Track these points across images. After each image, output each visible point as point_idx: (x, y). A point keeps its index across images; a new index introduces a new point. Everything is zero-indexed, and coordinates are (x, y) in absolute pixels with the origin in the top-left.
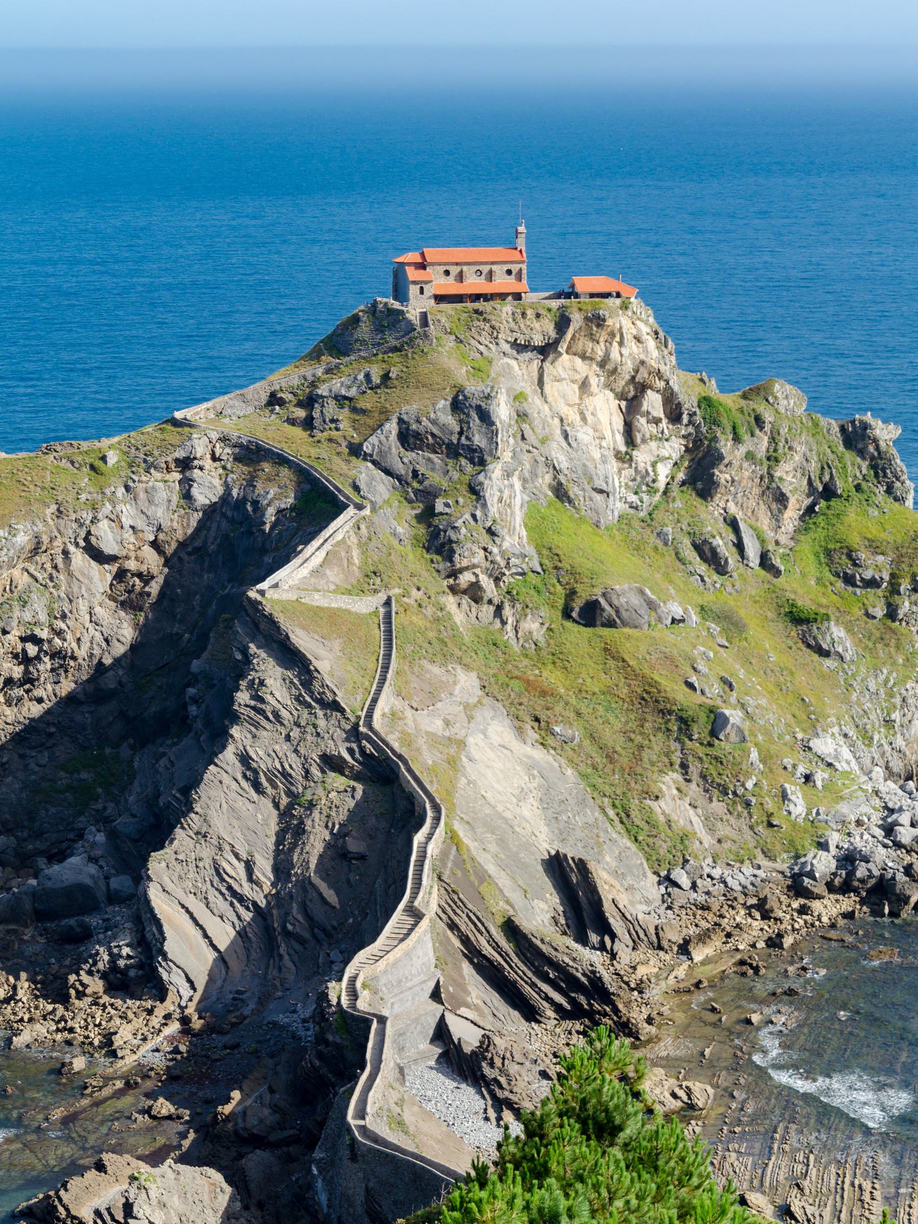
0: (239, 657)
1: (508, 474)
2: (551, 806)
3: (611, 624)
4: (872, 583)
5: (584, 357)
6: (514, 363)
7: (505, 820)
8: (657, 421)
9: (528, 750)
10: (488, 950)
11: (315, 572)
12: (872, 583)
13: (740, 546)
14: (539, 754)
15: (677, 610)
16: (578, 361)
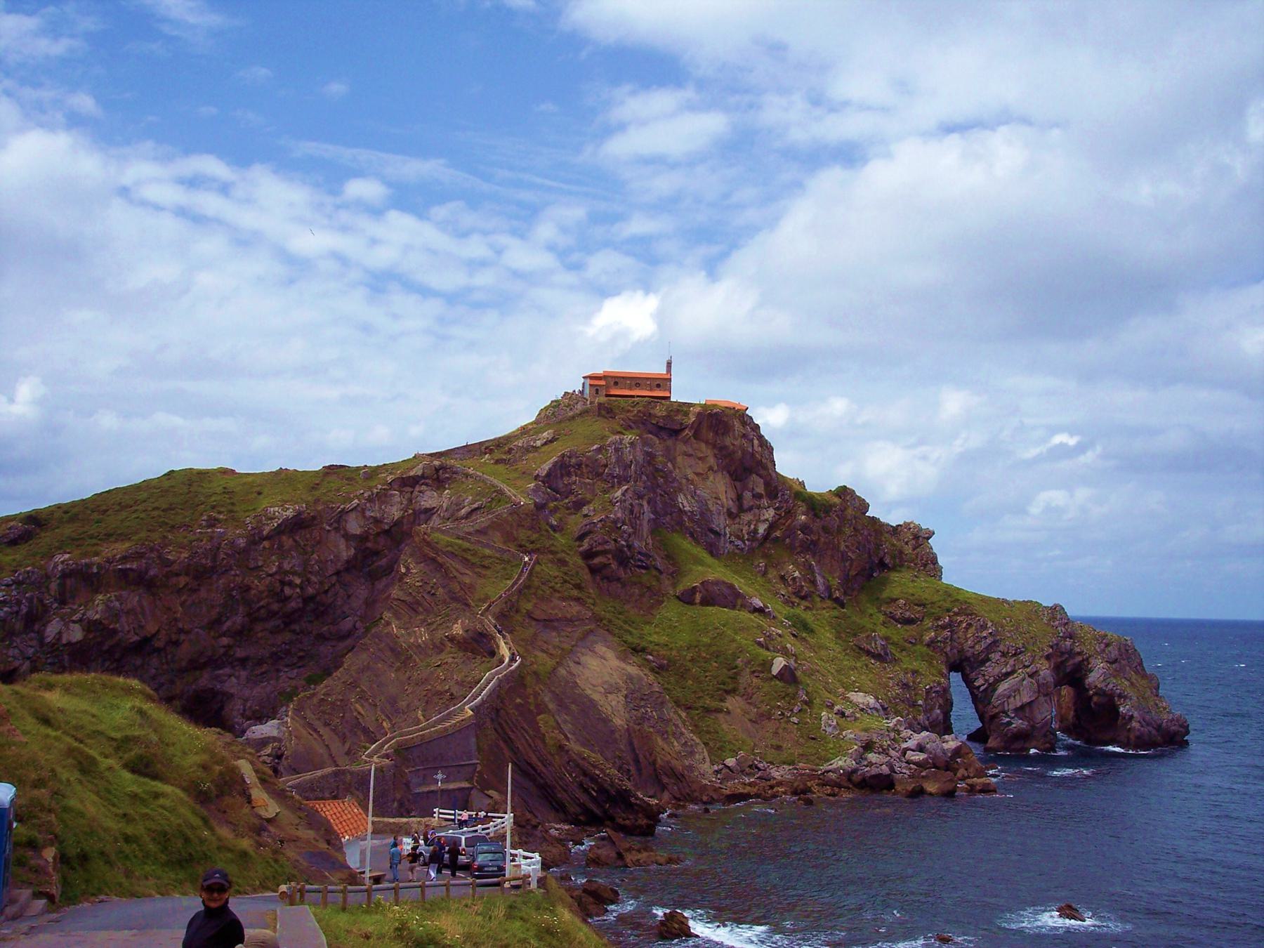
0: (403, 570)
1: (640, 497)
2: (635, 697)
3: (706, 602)
4: (909, 621)
5: (707, 443)
6: (655, 439)
7: (591, 701)
8: (759, 496)
9: (623, 665)
10: (534, 760)
12: (909, 621)
13: (813, 582)
14: (632, 670)
15: (758, 603)
16: (703, 446)
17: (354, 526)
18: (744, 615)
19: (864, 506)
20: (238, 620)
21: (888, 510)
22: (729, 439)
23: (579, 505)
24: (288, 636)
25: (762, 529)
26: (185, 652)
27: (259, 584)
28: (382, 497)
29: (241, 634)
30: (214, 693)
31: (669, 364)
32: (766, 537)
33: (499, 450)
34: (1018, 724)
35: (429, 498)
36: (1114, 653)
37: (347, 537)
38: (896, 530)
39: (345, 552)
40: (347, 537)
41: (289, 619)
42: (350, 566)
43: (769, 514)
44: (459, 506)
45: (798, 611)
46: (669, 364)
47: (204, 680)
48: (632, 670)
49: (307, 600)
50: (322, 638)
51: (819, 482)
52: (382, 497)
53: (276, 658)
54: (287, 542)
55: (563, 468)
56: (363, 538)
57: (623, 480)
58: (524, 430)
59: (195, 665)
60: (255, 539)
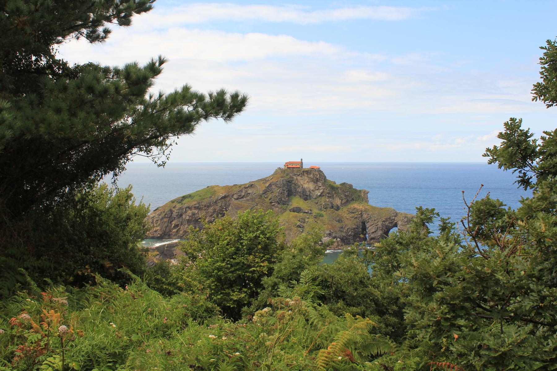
19: (351, 186)
21: (357, 186)
25: (319, 194)
28: (241, 191)
31: (302, 160)
32: (320, 196)
35: (250, 191)
38: (360, 191)
43: (321, 191)
46: (302, 160)
51: (338, 183)
52: (241, 191)
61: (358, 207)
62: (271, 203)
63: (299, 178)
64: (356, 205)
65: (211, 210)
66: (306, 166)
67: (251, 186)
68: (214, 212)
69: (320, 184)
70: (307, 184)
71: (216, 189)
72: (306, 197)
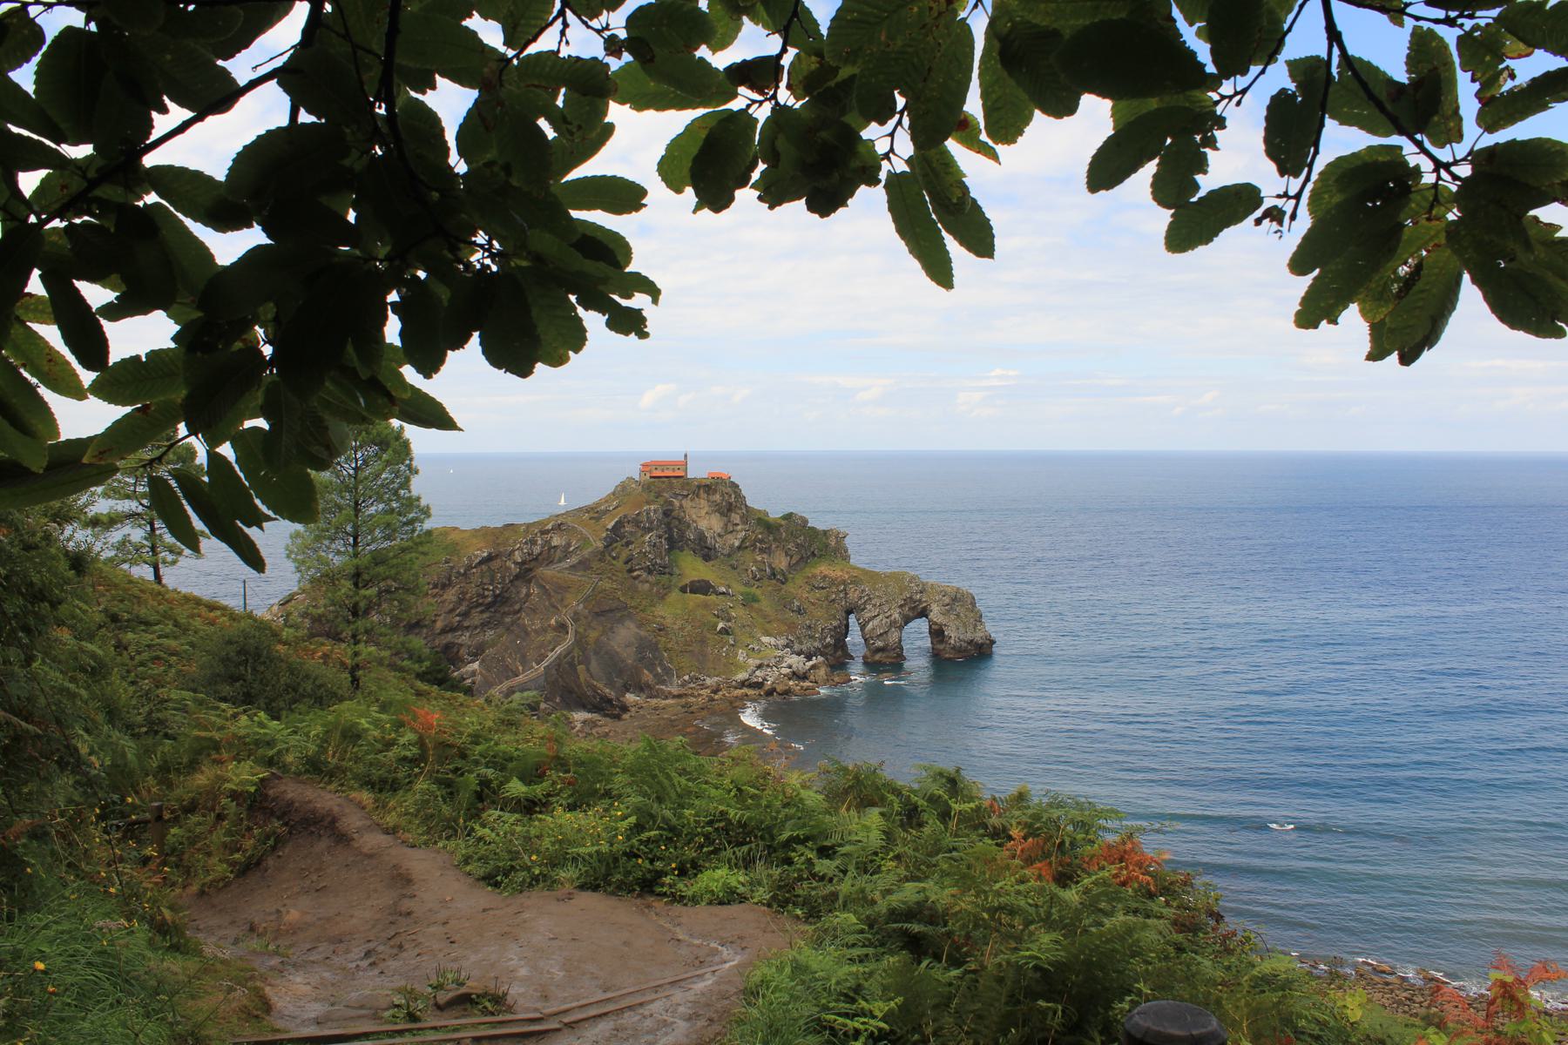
11: (573, 567)
17: (518, 557)
18: (713, 597)
19: (805, 521)
20: (463, 608)
21: (818, 523)
22: (723, 494)
23: (628, 544)
24: (485, 615)
26: (439, 625)
27: (473, 590)
29: (465, 615)
30: (454, 644)
32: (739, 548)
33: (595, 513)
34: (880, 644)
35: (556, 541)
36: (947, 600)
37: (516, 563)
38: (825, 532)
39: (515, 570)
40: (516, 563)
41: (489, 606)
42: (517, 577)
44: (569, 545)
45: (753, 590)
47: (449, 637)
48: (643, 633)
49: (496, 596)
50: (508, 614)
51: (775, 513)
53: (483, 625)
54: (484, 567)
55: (619, 525)
56: (524, 563)
57: (650, 530)
58: (607, 500)
59: (444, 631)
60: (470, 567)
61: (833, 574)
62: (631, 571)
63: (687, 503)
64: (823, 569)
65: (451, 595)
66: (696, 472)
67: (558, 528)
68: (461, 601)
69: (736, 518)
70: (707, 522)
71: (453, 536)
72: (706, 552)
